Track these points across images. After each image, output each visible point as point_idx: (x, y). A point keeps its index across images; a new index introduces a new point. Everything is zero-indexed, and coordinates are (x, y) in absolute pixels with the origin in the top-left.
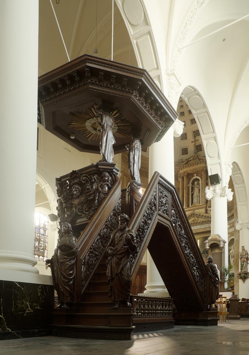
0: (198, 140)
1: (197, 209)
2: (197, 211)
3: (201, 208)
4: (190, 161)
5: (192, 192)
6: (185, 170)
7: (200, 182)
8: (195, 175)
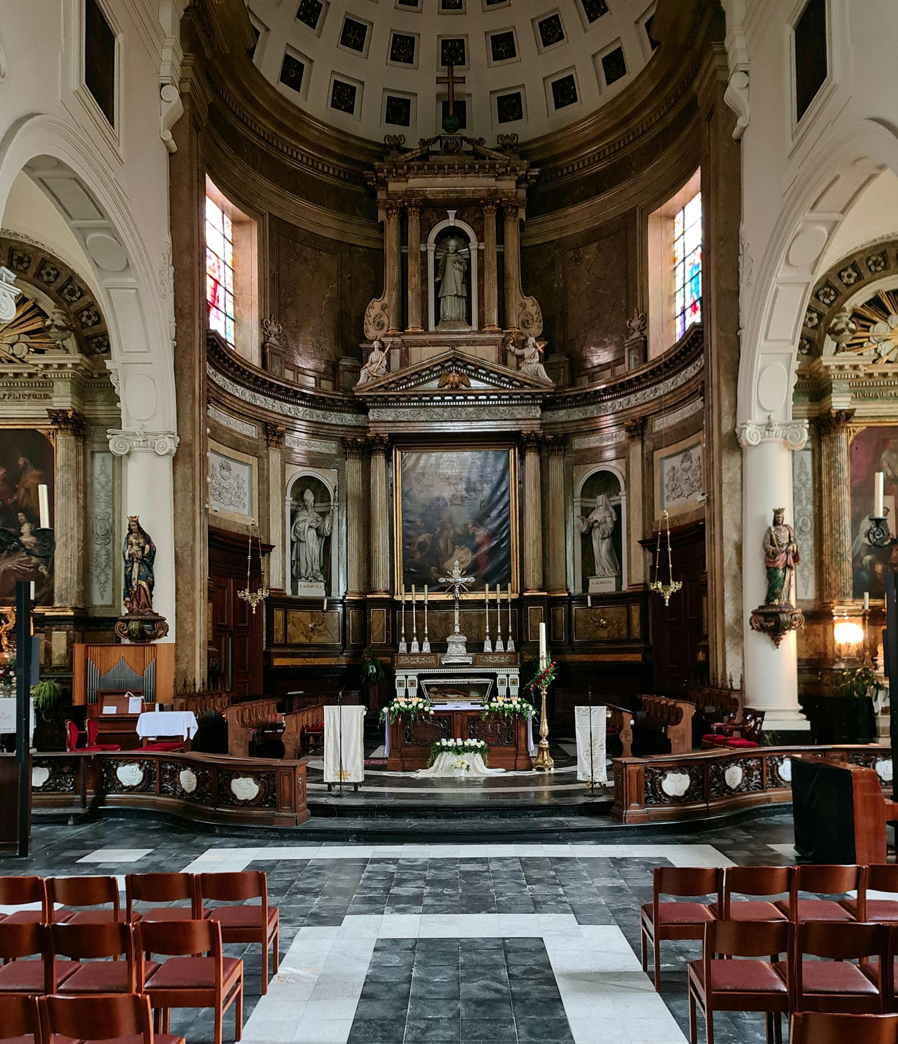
0: (462, 80)
1: (469, 343)
2: (469, 351)
3: (483, 343)
4: (435, 153)
5: (436, 276)
6: (414, 183)
7: (473, 245)
8: (452, 213)
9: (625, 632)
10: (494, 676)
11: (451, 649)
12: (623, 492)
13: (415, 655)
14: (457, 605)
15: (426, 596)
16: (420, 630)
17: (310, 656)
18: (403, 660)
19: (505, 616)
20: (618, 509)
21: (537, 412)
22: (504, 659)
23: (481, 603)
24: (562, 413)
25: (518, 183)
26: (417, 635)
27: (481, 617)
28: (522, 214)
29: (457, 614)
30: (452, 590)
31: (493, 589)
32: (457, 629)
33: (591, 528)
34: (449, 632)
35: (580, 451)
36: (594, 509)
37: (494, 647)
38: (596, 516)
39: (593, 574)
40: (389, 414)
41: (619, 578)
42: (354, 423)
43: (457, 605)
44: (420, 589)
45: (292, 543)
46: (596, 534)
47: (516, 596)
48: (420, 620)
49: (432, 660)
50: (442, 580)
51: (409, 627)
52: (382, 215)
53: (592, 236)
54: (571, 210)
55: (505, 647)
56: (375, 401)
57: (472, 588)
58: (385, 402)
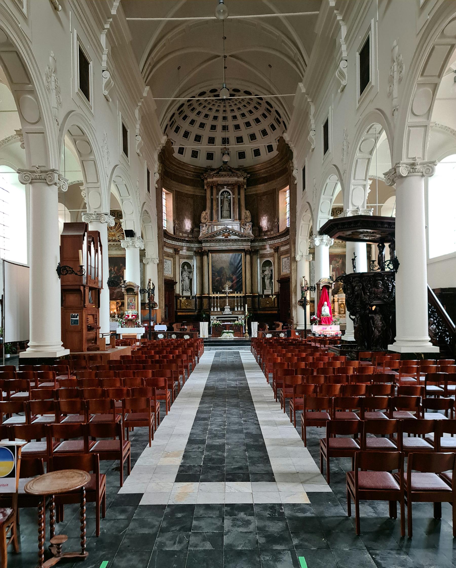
6: (215, 179)
8: (225, 187)
9: (273, 305)
10: (237, 317)
11: (226, 310)
12: (273, 267)
13: (216, 312)
14: (227, 298)
15: (219, 295)
16: (217, 304)
17: (187, 312)
18: (212, 313)
19: (241, 301)
20: (272, 270)
21: (249, 244)
22: (241, 313)
23: (234, 297)
24: (257, 243)
25: (244, 179)
26: (216, 306)
27: (234, 301)
28: (245, 187)
29: (227, 300)
30: (226, 293)
31: (237, 293)
32: (227, 304)
33: (264, 276)
34: (225, 305)
35: (261, 254)
36: (265, 270)
37: (238, 309)
38: (266, 273)
39: (265, 289)
40: (208, 244)
41: (272, 290)
42: (198, 246)
43: (227, 298)
44: (217, 293)
45: (182, 281)
46: (266, 278)
47: (244, 295)
48: (217, 302)
49: (220, 313)
50: (223, 291)
51: (214, 304)
52: (206, 187)
53: (265, 194)
54: (259, 186)
55: (241, 309)
56: (204, 241)
57: (231, 293)
58: (207, 241)
